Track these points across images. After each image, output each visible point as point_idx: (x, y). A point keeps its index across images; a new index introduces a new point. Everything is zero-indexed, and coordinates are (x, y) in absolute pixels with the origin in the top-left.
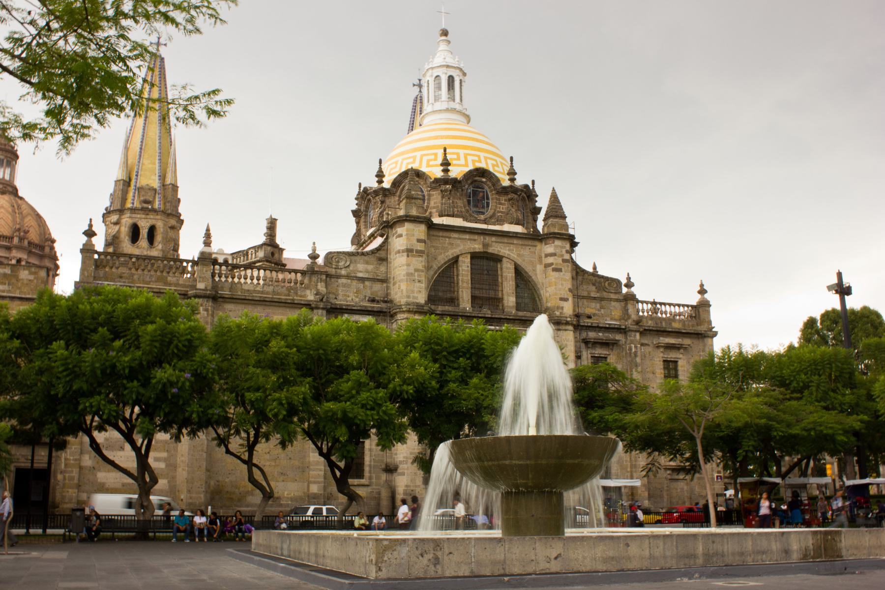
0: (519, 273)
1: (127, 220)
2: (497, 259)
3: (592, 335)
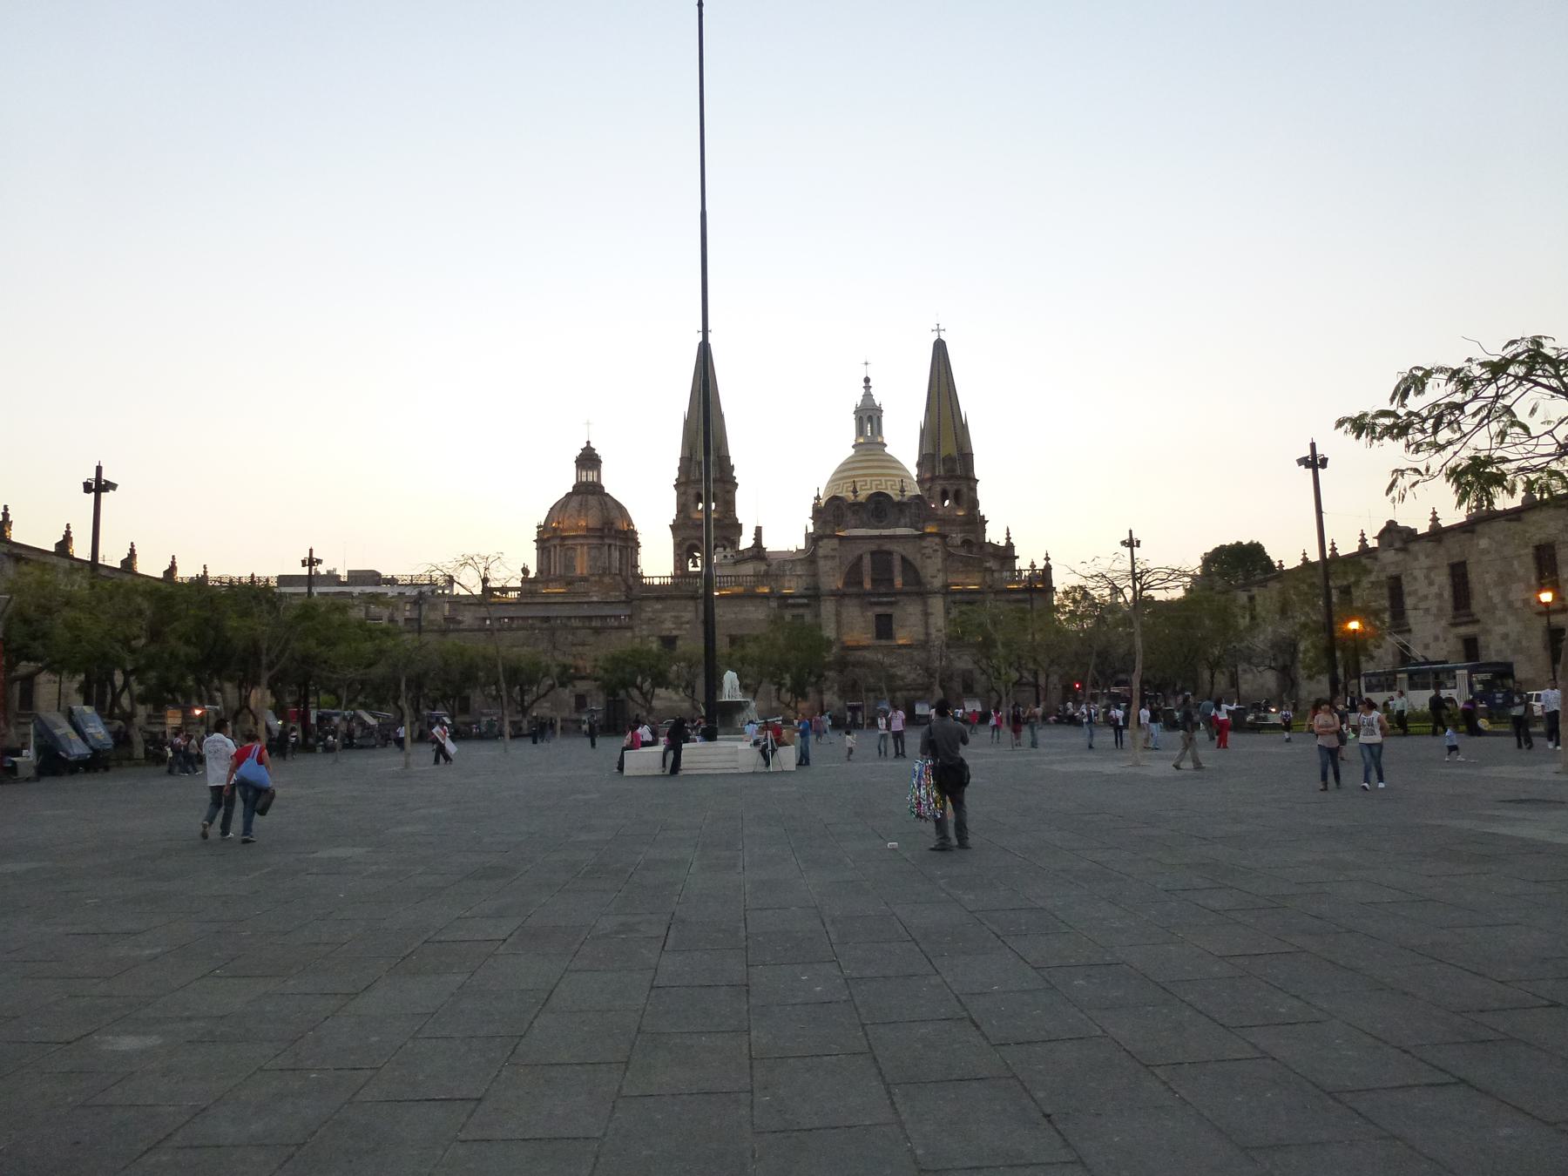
0: (904, 559)
1: (692, 492)
2: (890, 553)
3: (958, 597)
